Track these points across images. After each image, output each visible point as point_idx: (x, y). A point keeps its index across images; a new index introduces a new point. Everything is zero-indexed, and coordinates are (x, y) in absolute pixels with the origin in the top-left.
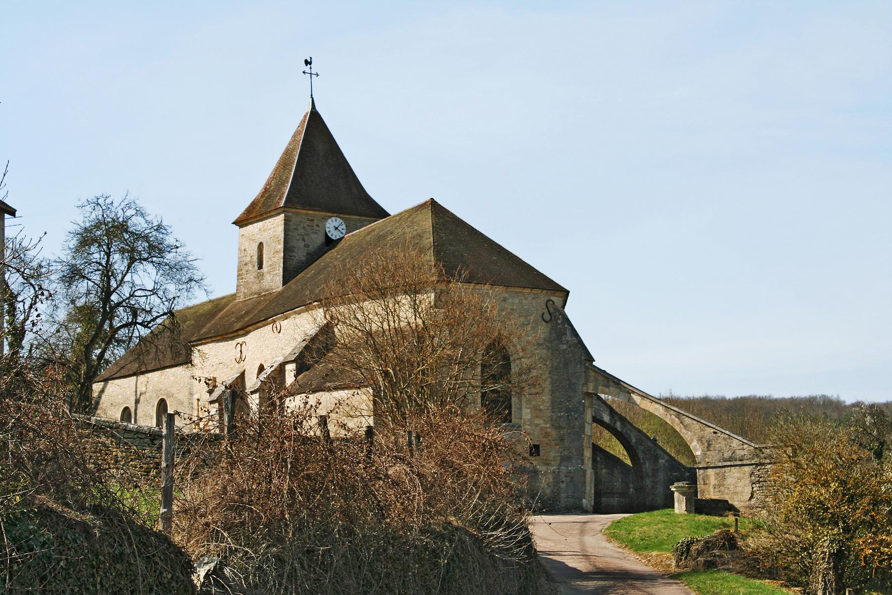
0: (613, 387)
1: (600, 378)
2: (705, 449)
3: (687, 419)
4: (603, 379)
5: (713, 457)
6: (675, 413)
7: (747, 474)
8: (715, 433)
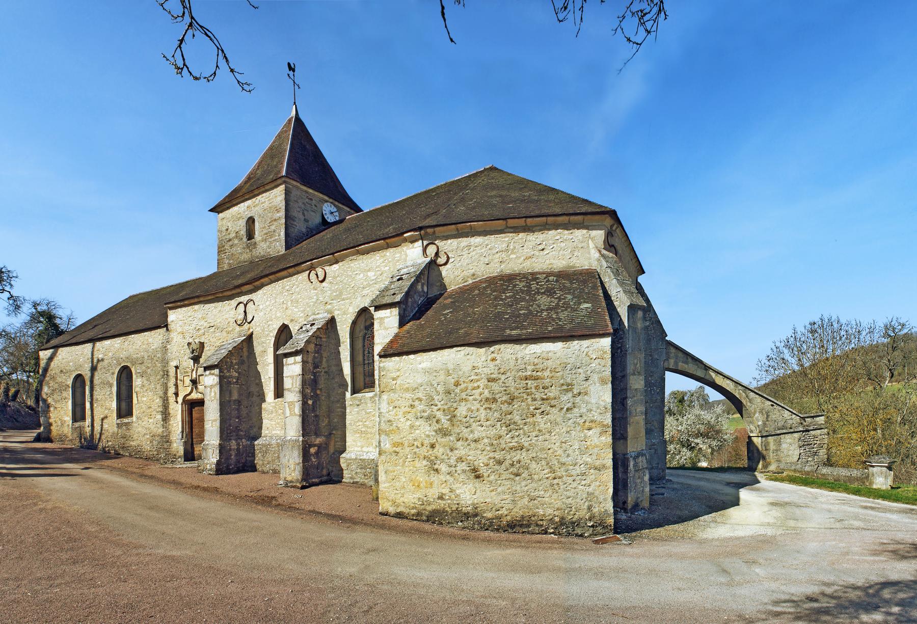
0: (692, 363)
1: (680, 354)
2: (765, 419)
3: (752, 393)
4: (682, 356)
5: (770, 426)
6: (742, 388)
7: (797, 440)
8: (772, 405)
